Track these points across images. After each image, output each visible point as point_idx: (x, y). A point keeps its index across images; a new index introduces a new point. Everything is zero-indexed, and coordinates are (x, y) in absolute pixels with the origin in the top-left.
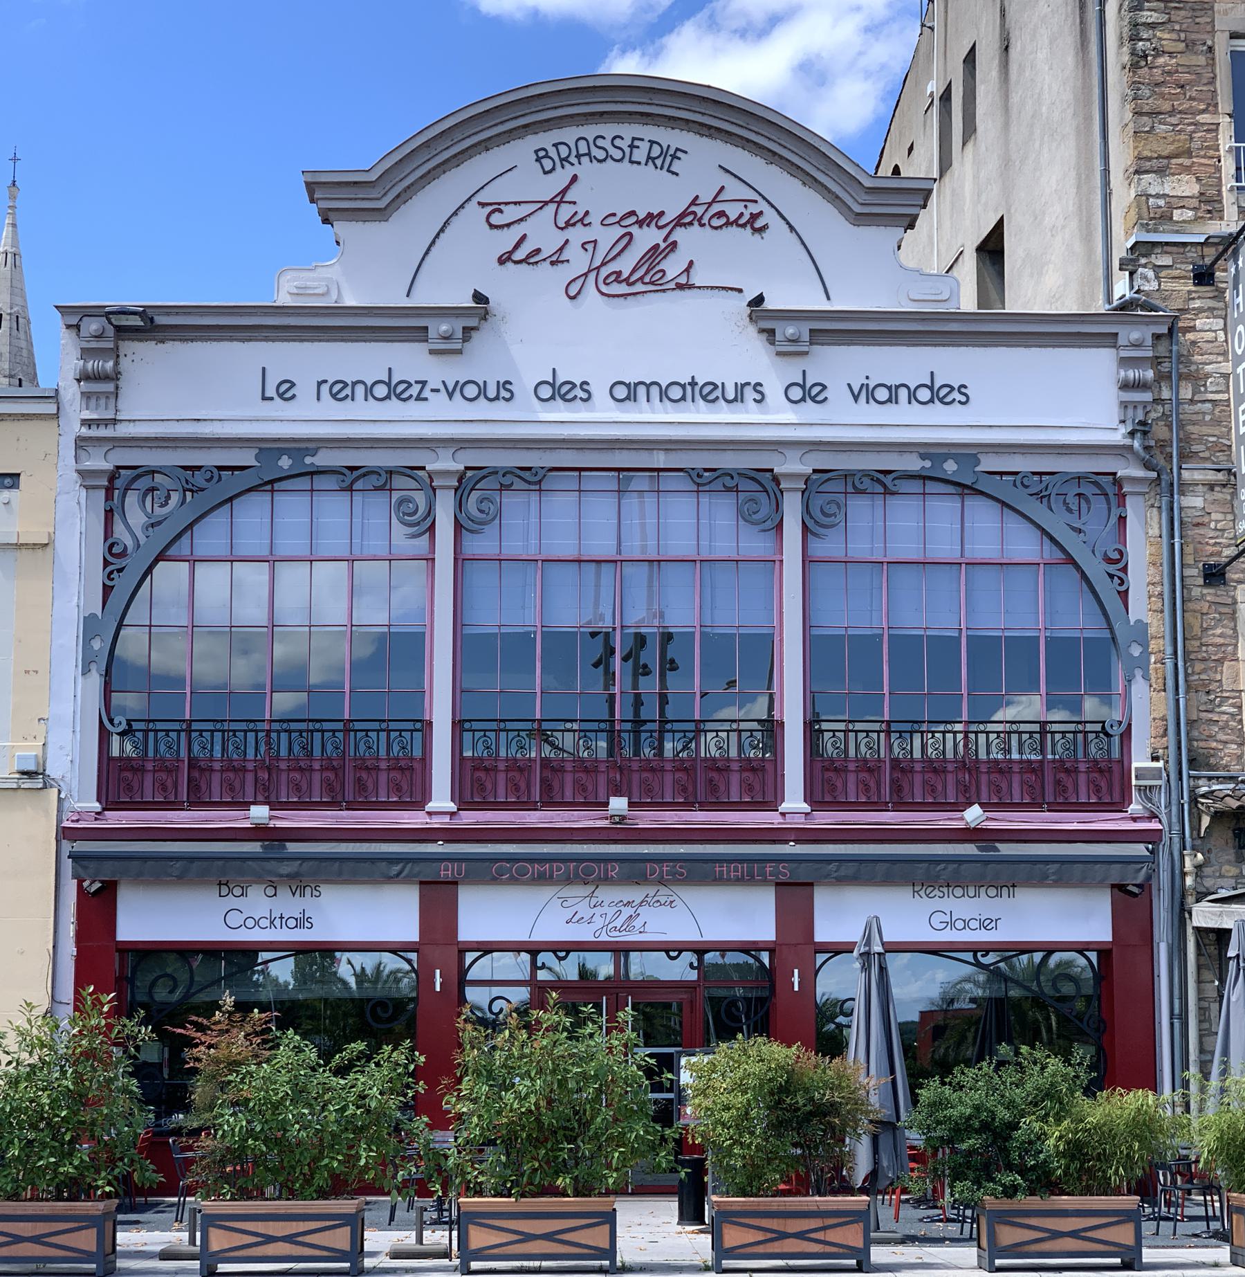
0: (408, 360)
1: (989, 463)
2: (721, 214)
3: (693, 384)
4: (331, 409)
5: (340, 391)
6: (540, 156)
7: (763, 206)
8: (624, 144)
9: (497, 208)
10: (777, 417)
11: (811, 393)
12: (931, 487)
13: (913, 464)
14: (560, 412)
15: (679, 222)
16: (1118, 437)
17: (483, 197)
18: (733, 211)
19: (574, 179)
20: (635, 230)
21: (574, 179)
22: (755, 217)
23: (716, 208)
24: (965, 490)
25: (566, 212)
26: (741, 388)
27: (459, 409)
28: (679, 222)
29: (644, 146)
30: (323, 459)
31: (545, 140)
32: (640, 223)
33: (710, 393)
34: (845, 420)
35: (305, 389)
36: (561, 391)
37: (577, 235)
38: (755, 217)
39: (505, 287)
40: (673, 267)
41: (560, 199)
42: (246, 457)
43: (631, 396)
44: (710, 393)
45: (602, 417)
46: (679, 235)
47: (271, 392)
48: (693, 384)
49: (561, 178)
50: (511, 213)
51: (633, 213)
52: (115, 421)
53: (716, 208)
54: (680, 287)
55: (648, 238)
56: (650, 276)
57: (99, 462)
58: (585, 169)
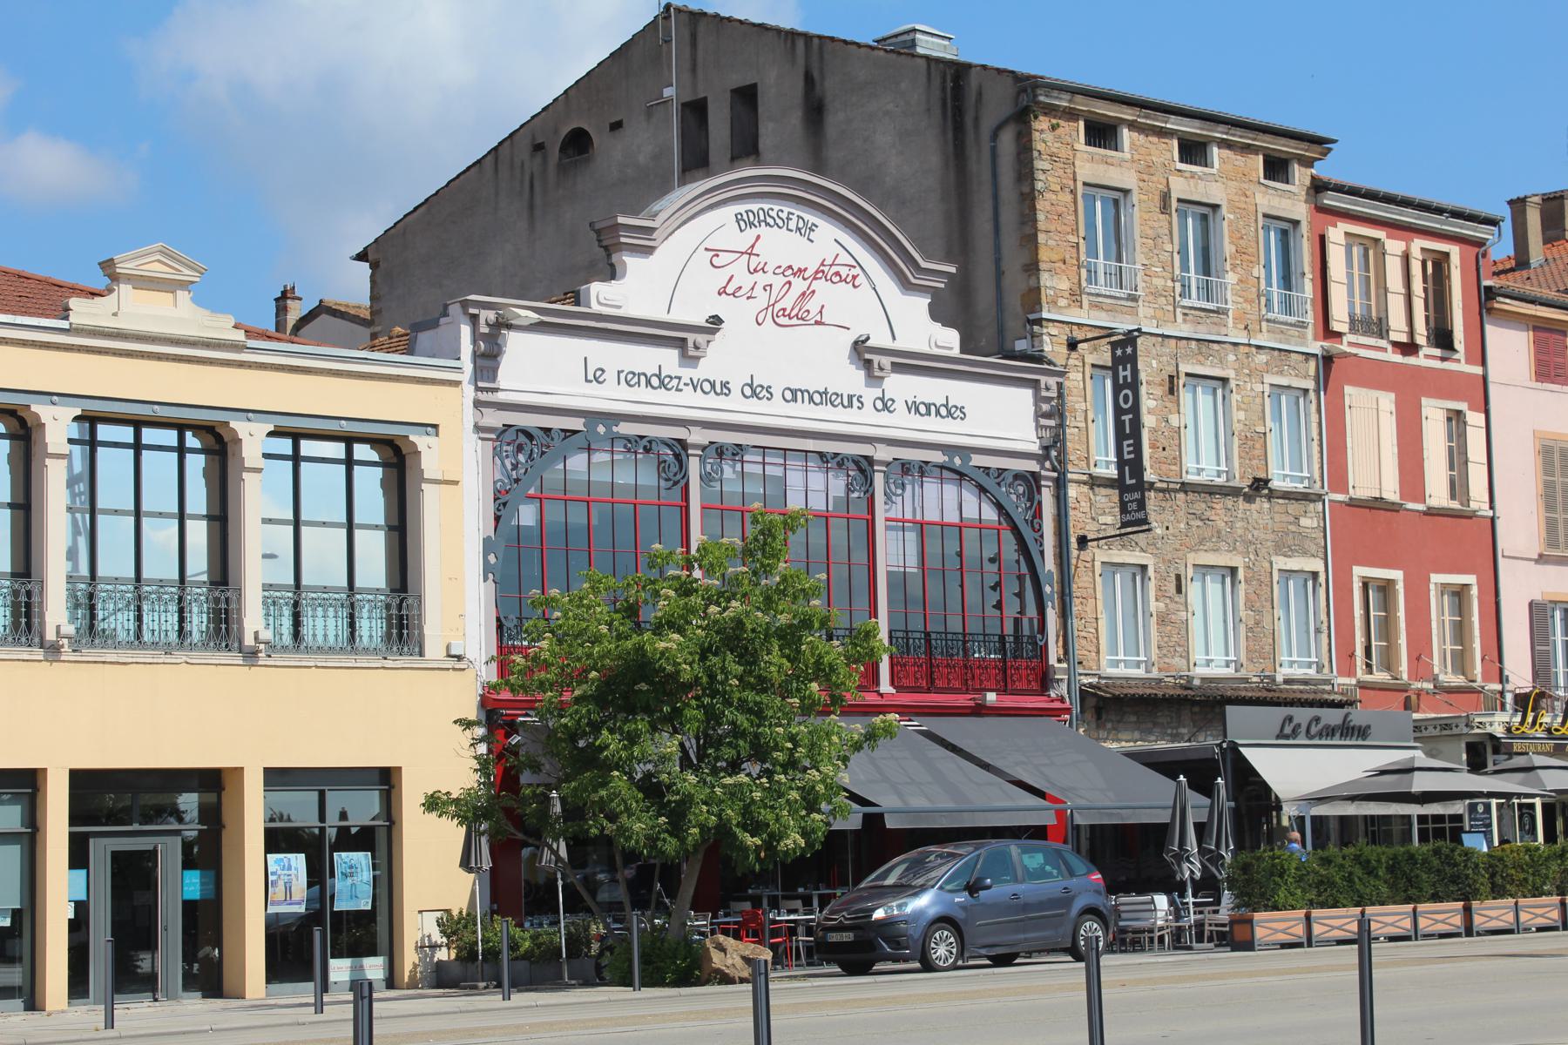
0: (668, 358)
1: (977, 460)
2: (837, 274)
3: (826, 392)
4: (624, 392)
5: (633, 379)
6: (738, 218)
7: (857, 271)
8: (784, 216)
9: (716, 253)
10: (865, 420)
11: (886, 405)
12: (946, 474)
13: (937, 457)
14: (754, 405)
15: (819, 274)
16: (1035, 448)
17: (707, 244)
18: (844, 271)
19: (758, 237)
20: (791, 278)
21: (758, 237)
22: (854, 277)
23: (834, 269)
24: (961, 476)
25: (754, 261)
26: (850, 397)
27: (699, 399)
28: (819, 274)
29: (795, 218)
30: (625, 429)
31: (741, 208)
32: (794, 274)
33: (826, 397)
34: (901, 424)
35: (610, 376)
36: (754, 391)
37: (762, 279)
38: (854, 277)
39: (737, 314)
40: (813, 305)
41: (750, 253)
42: (577, 424)
43: (795, 399)
44: (826, 397)
45: (774, 412)
46: (816, 285)
47: (591, 377)
48: (826, 392)
49: (751, 234)
50: (723, 259)
51: (790, 267)
52: (496, 390)
53: (834, 269)
54: (817, 323)
55: (799, 285)
56: (795, 317)
57: (495, 419)
58: (763, 230)
